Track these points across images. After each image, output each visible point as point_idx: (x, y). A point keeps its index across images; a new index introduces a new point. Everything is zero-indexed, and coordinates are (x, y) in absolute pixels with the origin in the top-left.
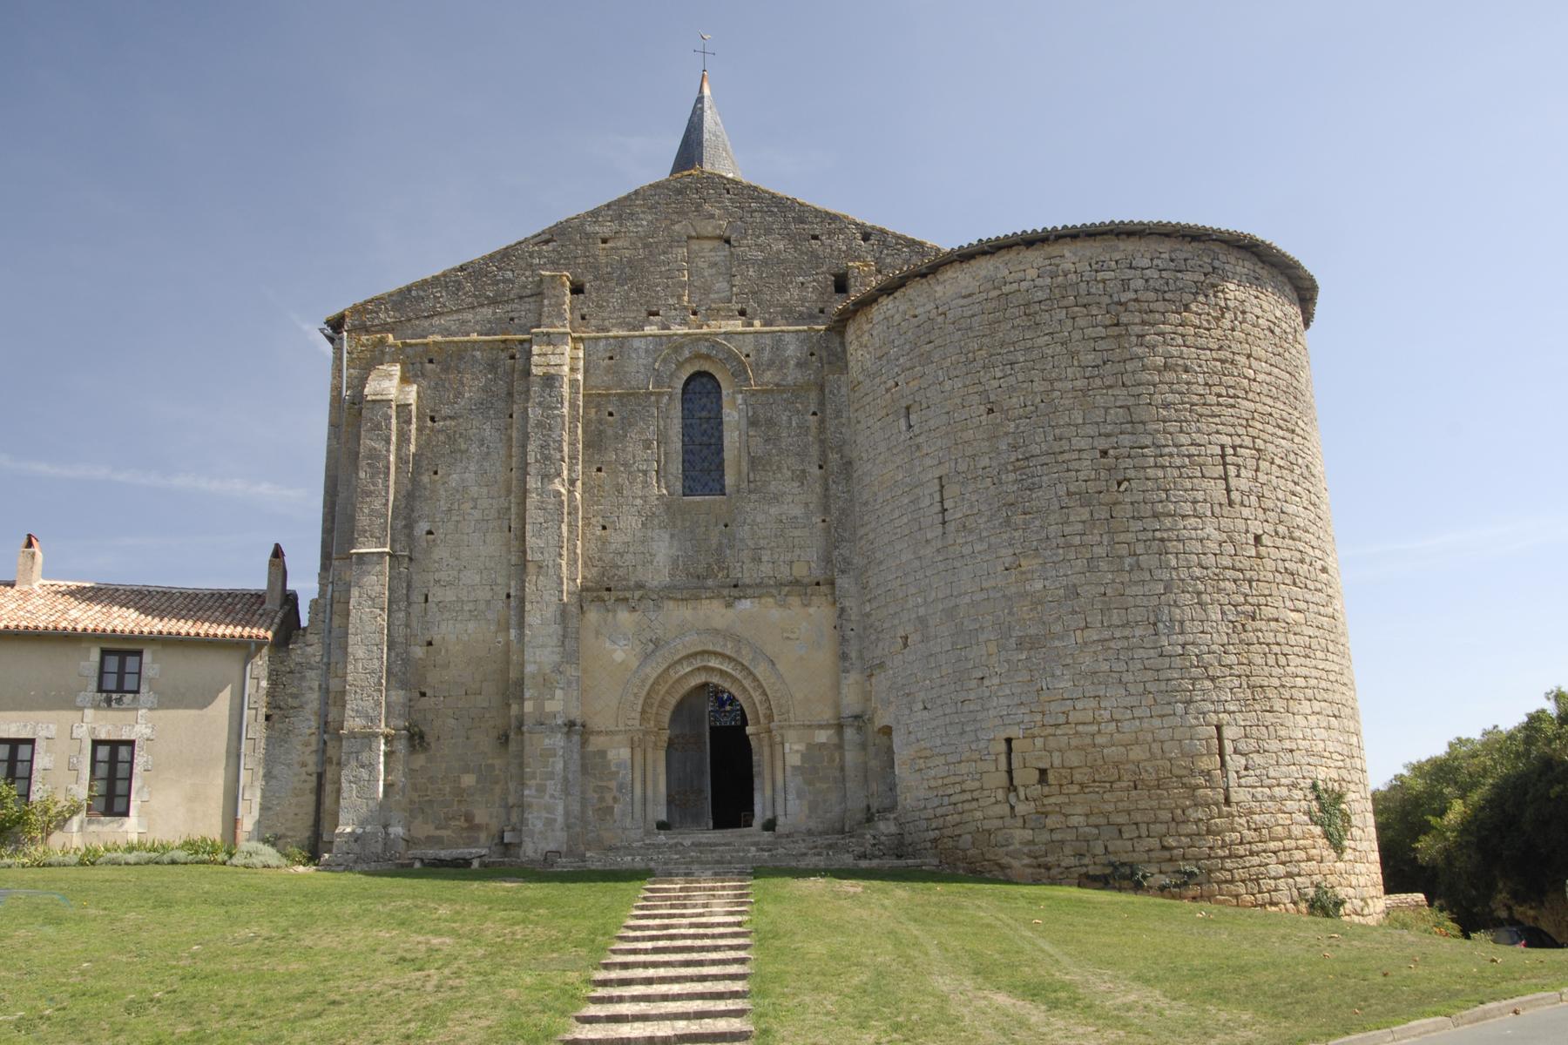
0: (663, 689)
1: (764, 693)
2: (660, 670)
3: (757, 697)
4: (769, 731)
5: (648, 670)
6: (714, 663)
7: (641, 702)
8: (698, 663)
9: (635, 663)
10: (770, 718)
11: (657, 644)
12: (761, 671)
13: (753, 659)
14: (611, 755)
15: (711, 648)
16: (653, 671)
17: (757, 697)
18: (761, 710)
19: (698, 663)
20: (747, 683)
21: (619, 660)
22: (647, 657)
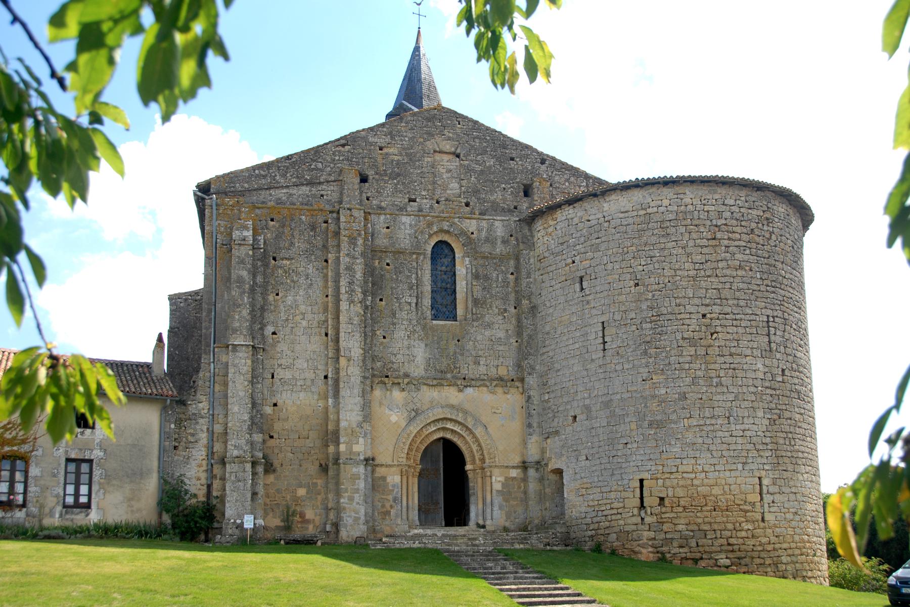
1: (479, 445)
3: (475, 448)
4: (483, 469)
5: (411, 428)
6: (449, 425)
7: (407, 447)
8: (440, 425)
9: (403, 424)
10: (483, 460)
12: (479, 432)
13: (475, 424)
14: (389, 479)
15: (449, 416)
16: (414, 429)
17: (475, 448)
18: (477, 456)
19: (440, 425)
20: (469, 438)
22: (411, 420)
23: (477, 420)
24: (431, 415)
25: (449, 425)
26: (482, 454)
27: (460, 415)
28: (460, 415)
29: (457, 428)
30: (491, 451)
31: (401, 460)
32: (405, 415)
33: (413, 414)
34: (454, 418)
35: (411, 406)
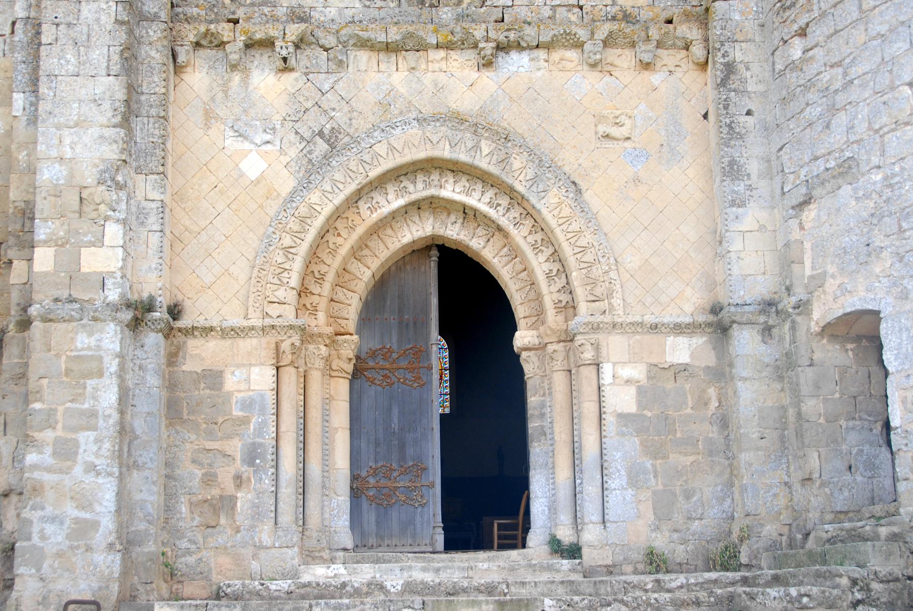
0: (345, 243)
1: (557, 256)
3: (540, 265)
6: (452, 190)
8: (418, 190)
10: (569, 308)
11: (332, 138)
12: (551, 205)
13: (535, 180)
15: (445, 152)
17: (540, 265)
18: (550, 295)
19: (418, 190)
22: (311, 171)
23: (545, 166)
24: (381, 149)
25: (452, 190)
26: (568, 289)
27: (486, 147)
28: (486, 147)
29: (478, 199)
30: (597, 272)
32: (293, 152)
33: (321, 146)
34: (463, 157)
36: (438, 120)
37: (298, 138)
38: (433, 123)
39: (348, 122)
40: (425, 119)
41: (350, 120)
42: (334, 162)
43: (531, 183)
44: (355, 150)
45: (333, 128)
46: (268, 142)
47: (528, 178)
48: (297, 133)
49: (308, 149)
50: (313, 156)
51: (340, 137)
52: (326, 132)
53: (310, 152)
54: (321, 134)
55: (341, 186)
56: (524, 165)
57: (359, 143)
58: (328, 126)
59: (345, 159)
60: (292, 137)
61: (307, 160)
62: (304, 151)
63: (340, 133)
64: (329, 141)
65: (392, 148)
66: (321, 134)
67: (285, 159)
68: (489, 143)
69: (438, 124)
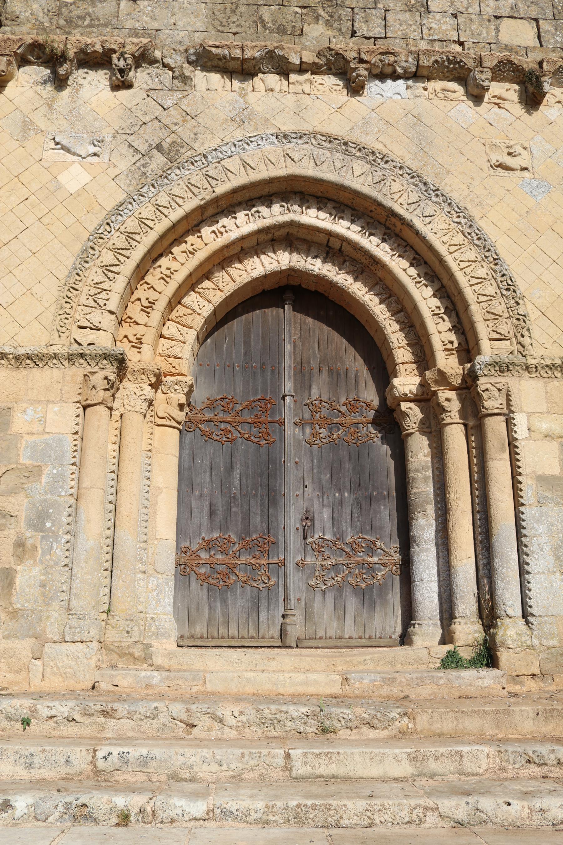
2: (176, 215)
14: (21, 421)
21: (73, 187)
22: (145, 183)
24: (233, 164)
31: (85, 337)
35: (153, 134)
36: (301, 137)
37: (131, 150)
38: (294, 140)
39: (192, 136)
40: (285, 136)
41: (195, 134)
42: (173, 175)
43: (413, 206)
44: (200, 163)
45: (174, 142)
46: (95, 155)
47: (410, 202)
48: (130, 145)
49: (142, 162)
50: (149, 169)
51: (182, 151)
52: (165, 146)
53: (144, 166)
54: (159, 147)
55: (180, 201)
56: (405, 188)
57: (205, 157)
58: (168, 140)
59: (187, 172)
60: (124, 149)
61: (140, 173)
62: (138, 164)
63: (182, 147)
64: (168, 154)
65: (245, 164)
66: (159, 147)
67: (113, 172)
68: (362, 163)
69: (300, 142)
